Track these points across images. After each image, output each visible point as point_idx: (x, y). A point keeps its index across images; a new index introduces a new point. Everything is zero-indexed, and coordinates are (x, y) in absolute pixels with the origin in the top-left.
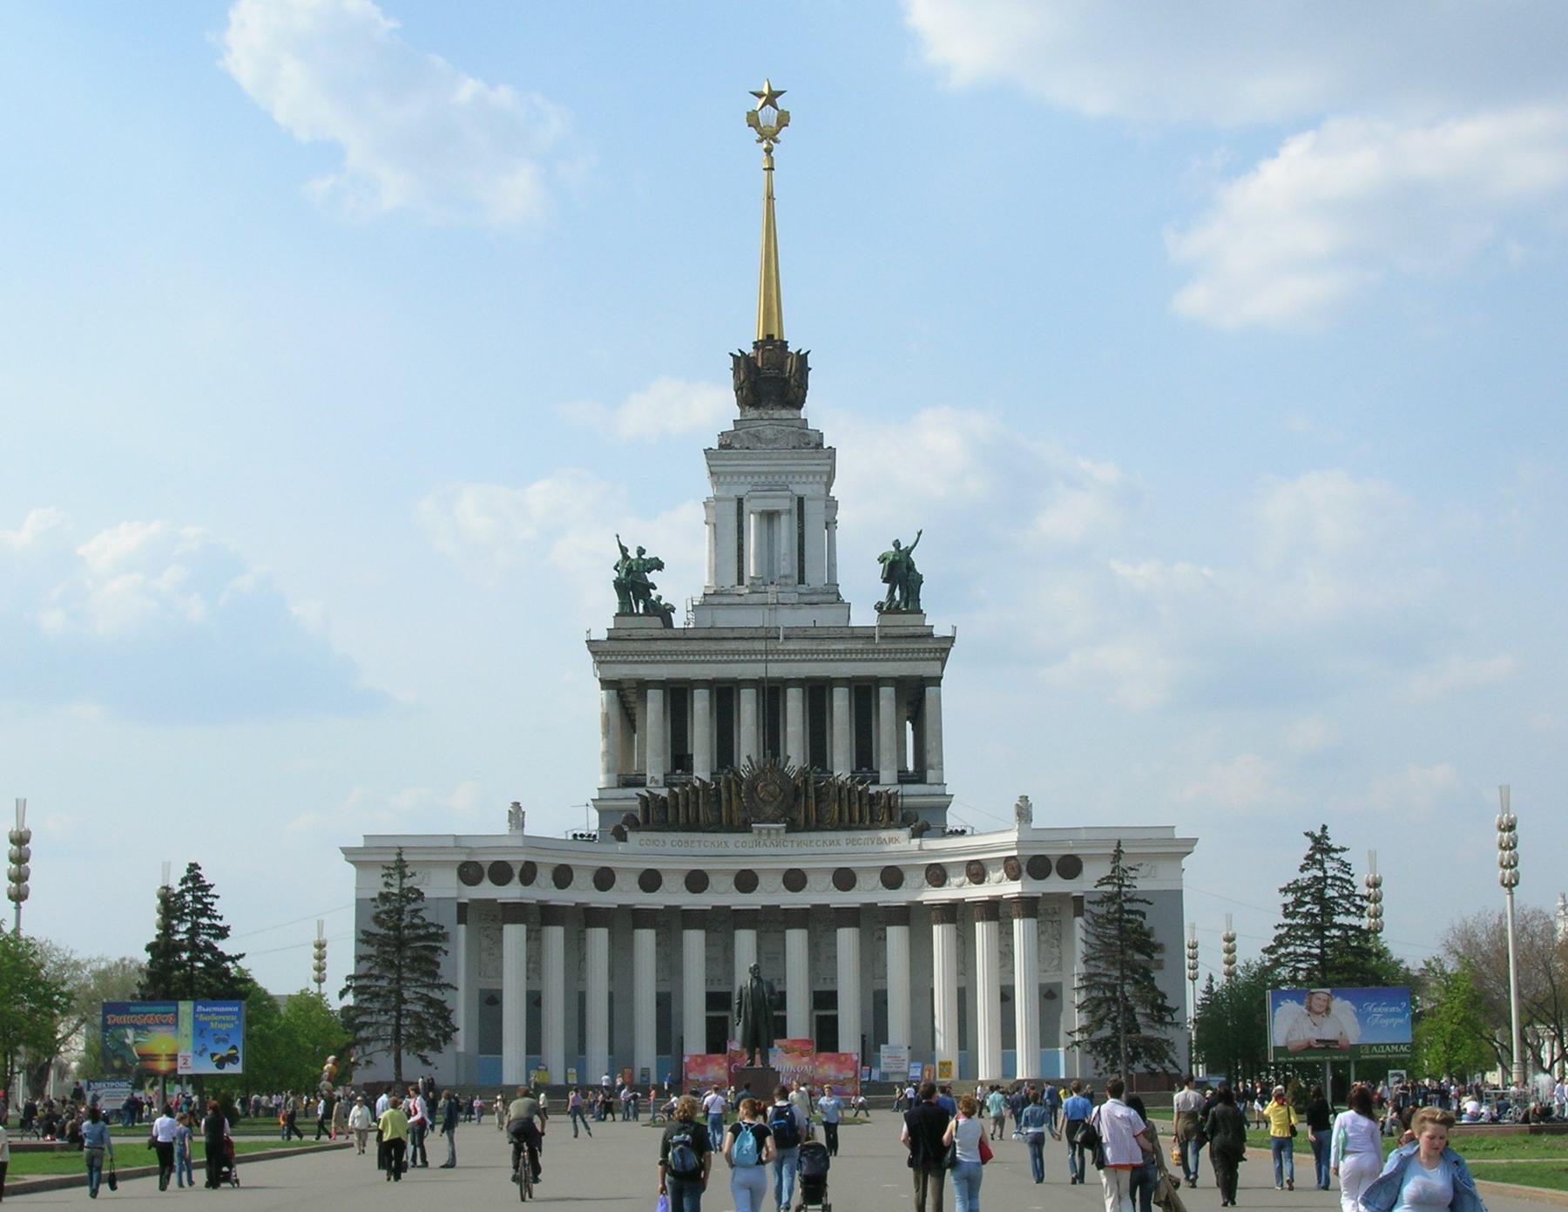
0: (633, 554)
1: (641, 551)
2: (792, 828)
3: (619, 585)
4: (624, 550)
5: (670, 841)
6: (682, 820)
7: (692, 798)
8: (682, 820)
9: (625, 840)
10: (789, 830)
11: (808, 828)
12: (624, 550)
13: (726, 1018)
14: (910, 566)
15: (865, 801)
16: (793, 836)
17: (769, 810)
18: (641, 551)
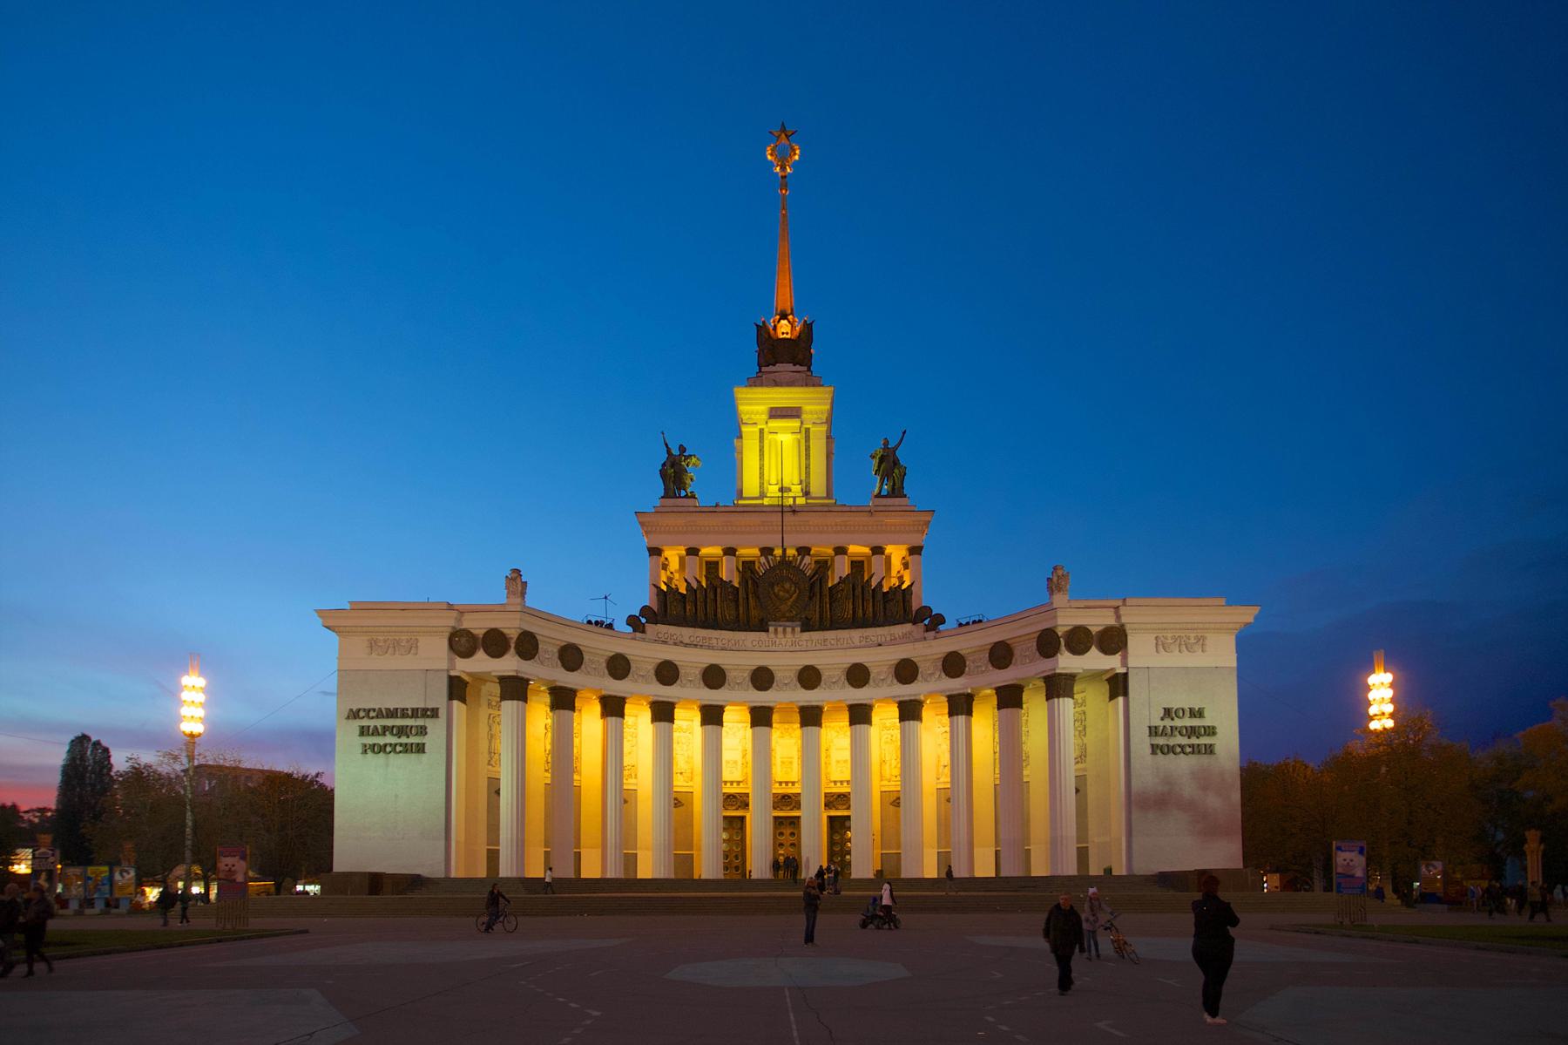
0: (676, 452)
1: (682, 449)
2: (807, 627)
3: (663, 474)
4: (669, 451)
5: (686, 633)
6: (701, 615)
7: (711, 595)
8: (701, 615)
9: (643, 632)
10: (802, 631)
11: (822, 628)
12: (669, 451)
13: (742, 819)
14: (896, 463)
15: (879, 597)
16: (806, 635)
17: (784, 608)
18: (682, 449)
